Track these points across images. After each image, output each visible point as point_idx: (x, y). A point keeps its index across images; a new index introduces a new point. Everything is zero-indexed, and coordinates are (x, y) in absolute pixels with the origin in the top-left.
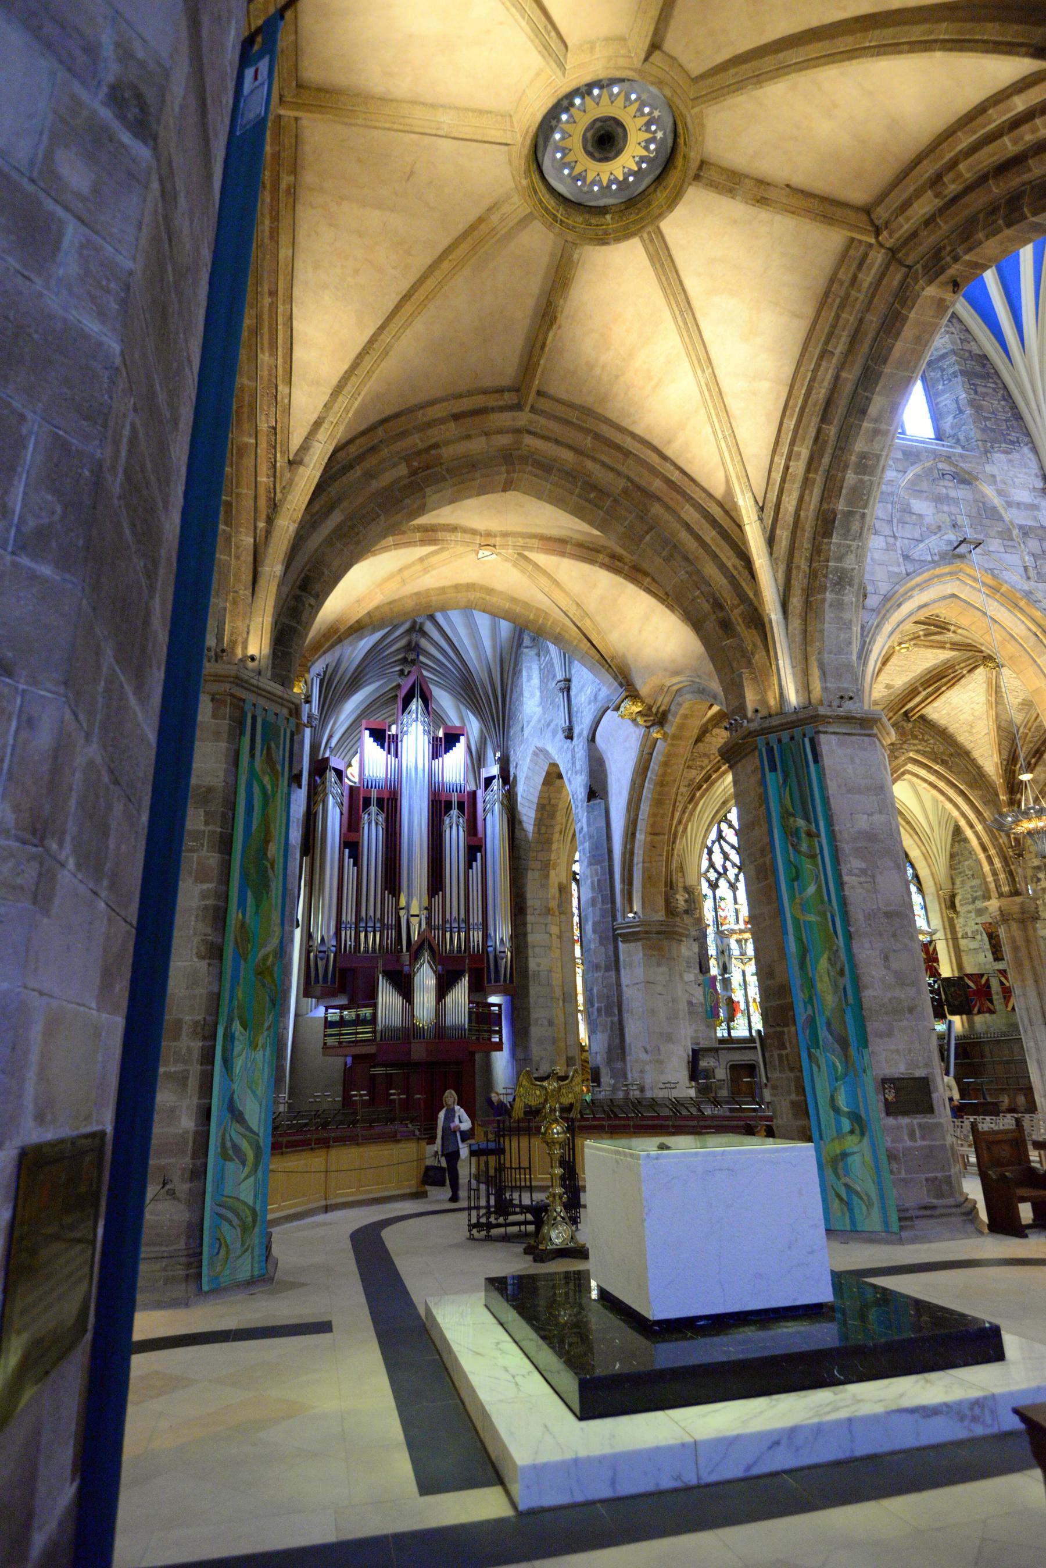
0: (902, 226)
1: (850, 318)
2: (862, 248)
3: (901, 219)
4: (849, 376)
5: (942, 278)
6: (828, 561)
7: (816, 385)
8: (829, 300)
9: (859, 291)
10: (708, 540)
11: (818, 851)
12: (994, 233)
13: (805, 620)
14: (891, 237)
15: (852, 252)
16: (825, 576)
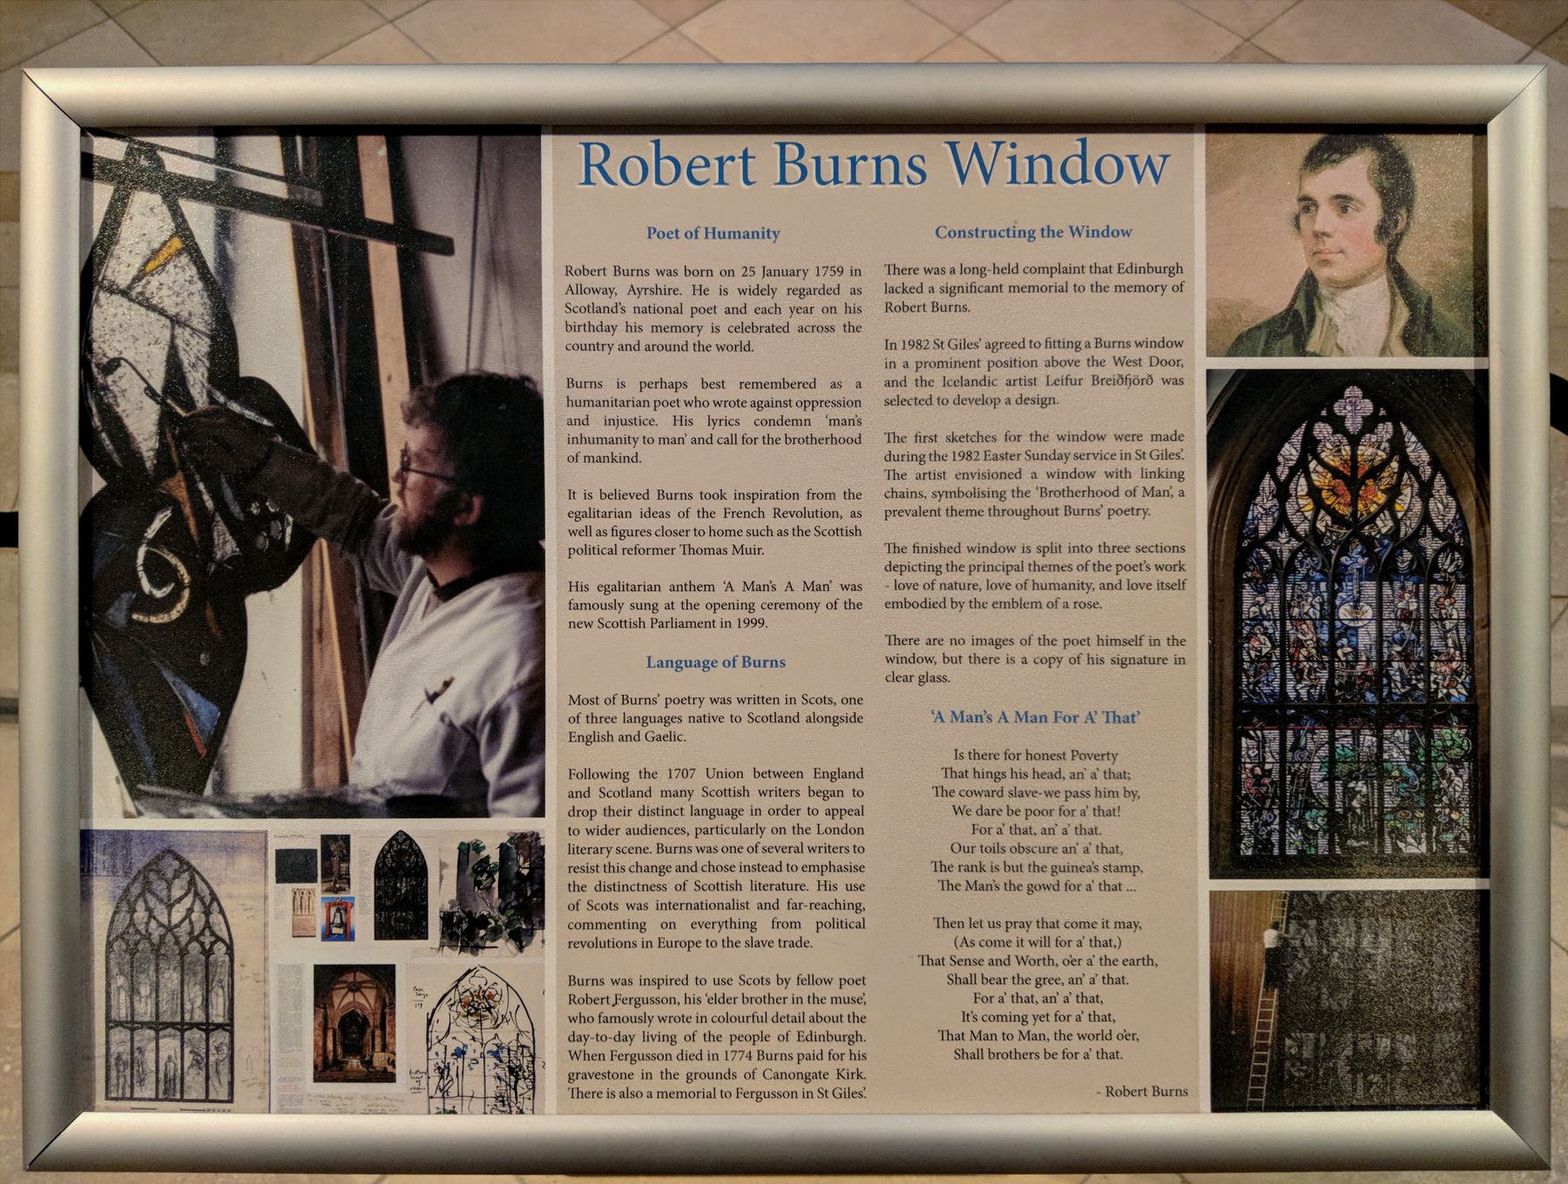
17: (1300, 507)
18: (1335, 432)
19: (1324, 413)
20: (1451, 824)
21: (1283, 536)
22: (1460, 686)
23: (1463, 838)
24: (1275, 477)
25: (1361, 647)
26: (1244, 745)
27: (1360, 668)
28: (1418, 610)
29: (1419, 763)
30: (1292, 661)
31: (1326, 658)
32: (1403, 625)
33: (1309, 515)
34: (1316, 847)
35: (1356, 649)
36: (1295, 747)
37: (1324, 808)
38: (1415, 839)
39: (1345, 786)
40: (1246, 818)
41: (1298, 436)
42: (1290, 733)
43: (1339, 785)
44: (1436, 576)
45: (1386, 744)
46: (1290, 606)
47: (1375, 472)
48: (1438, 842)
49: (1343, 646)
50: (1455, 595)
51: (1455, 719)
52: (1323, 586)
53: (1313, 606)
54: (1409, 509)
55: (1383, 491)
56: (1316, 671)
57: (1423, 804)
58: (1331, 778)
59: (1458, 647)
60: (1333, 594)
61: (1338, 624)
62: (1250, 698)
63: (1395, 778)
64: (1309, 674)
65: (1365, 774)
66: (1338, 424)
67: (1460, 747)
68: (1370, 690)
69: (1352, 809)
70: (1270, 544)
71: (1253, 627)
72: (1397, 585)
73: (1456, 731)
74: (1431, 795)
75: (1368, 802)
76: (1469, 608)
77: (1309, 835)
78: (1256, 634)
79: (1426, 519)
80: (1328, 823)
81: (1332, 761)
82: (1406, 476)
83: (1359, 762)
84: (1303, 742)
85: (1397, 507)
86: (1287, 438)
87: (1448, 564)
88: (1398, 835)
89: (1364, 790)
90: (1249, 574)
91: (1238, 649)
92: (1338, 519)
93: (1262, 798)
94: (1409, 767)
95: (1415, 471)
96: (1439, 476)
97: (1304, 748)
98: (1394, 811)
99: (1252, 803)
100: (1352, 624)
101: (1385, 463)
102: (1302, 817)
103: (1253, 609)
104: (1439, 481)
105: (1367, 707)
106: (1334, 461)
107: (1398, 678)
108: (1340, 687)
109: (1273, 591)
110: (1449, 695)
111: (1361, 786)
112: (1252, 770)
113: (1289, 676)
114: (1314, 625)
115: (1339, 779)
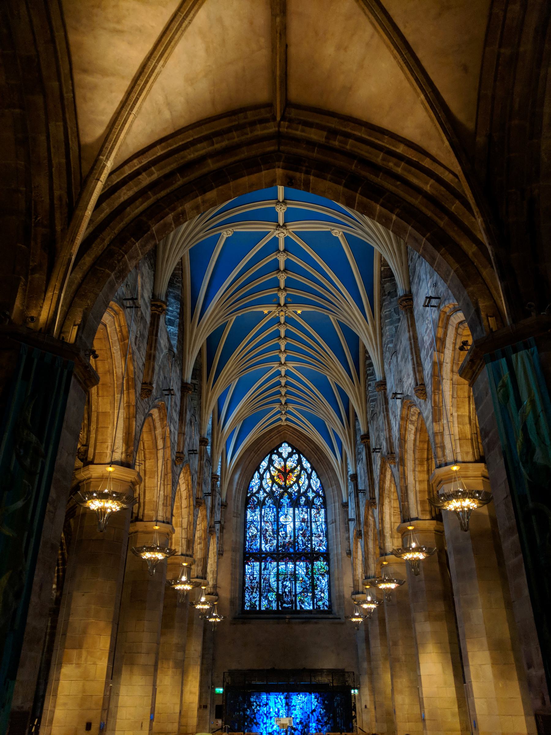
0: (297, 130)
1: (236, 138)
2: (268, 115)
3: (300, 127)
4: (211, 165)
5: (291, 173)
6: (126, 253)
7: (192, 149)
8: (233, 117)
9: (251, 132)
10: (55, 162)
11: (38, 471)
12: (336, 182)
13: (84, 278)
14: (287, 128)
15: (263, 110)
16: (119, 261)
18: (279, 458)
19: (275, 451)
20: (321, 599)
21: (261, 492)
23: (326, 604)
24: (259, 473)
25: (288, 531)
26: (247, 568)
28: (308, 518)
29: (309, 575)
31: (275, 536)
33: (270, 485)
34: (272, 607)
35: (286, 533)
36: (265, 568)
37: (275, 592)
38: (308, 603)
39: (282, 583)
40: (247, 596)
41: (267, 459)
42: (263, 563)
43: (280, 582)
44: (314, 506)
46: (264, 517)
47: (292, 470)
48: (317, 605)
49: (281, 531)
51: (322, 558)
52: (275, 510)
53: (271, 517)
54: (304, 483)
58: (278, 580)
59: (322, 531)
61: (280, 523)
62: (249, 550)
63: (301, 580)
64: (270, 541)
65: (290, 579)
66: (280, 455)
67: (324, 569)
68: (291, 547)
69: (285, 592)
70: (257, 495)
71: (251, 524)
72: (300, 509)
73: (322, 562)
74: (314, 587)
75: (291, 589)
76: (326, 518)
77: (270, 602)
79: (309, 486)
80: (277, 598)
81: (278, 574)
82: (302, 472)
84: (267, 567)
85: (300, 482)
86: (263, 459)
88: (302, 602)
89: (289, 585)
90: (250, 506)
91: (245, 532)
93: (253, 588)
94: (306, 576)
95: (305, 470)
96: (314, 472)
97: (268, 569)
98: (300, 593)
99: (249, 590)
100: (284, 524)
101: (296, 467)
102: (267, 595)
103: (251, 518)
104: (314, 474)
105: (291, 554)
106: (279, 467)
107: (301, 543)
108: (281, 546)
109: (258, 511)
110: (319, 549)
111: (288, 584)
112: (249, 577)
113: (263, 542)
114: (272, 524)
115: (280, 581)
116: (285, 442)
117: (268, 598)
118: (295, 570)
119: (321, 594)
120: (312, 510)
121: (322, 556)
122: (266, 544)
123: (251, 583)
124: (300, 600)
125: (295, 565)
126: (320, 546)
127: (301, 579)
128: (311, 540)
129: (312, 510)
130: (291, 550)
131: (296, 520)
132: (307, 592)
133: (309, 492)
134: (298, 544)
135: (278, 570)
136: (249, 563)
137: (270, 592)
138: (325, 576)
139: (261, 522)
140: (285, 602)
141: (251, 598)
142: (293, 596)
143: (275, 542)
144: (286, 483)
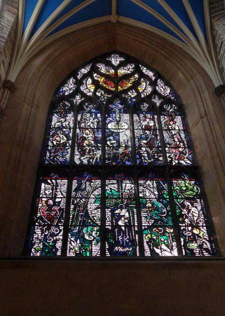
17: (88, 88)
20: (194, 238)
21: (78, 97)
22: (185, 159)
25: (121, 140)
26: (43, 187)
27: (121, 150)
28: (155, 125)
30: (78, 147)
32: (146, 131)
34: (91, 252)
35: (118, 142)
36: (78, 189)
37: (97, 225)
38: (168, 246)
39: (112, 212)
40: (38, 231)
42: (75, 182)
45: (141, 188)
46: (80, 123)
49: (110, 140)
50: (175, 120)
52: (99, 115)
53: (92, 123)
54: (145, 89)
55: (130, 84)
56: (93, 151)
57: (172, 224)
58: (103, 207)
59: (181, 141)
60: (104, 119)
63: (149, 207)
66: (109, 64)
68: (128, 160)
72: (142, 116)
74: (177, 219)
75: (129, 221)
78: (58, 134)
79: (155, 92)
82: (142, 79)
83: (122, 198)
85: (139, 89)
86: (84, 66)
87: (170, 109)
88: (154, 243)
89: (127, 215)
92: (107, 91)
93: (51, 219)
94: (158, 200)
95: (147, 78)
99: (45, 222)
101: (132, 74)
103: (58, 124)
107: (146, 155)
108: (109, 159)
109: (70, 117)
110: (179, 162)
111: (124, 212)
112: (46, 202)
113: (77, 152)
115: (108, 208)
116: (115, 52)
117: (83, 237)
118: (138, 192)
119: (192, 229)
120: (162, 117)
121: (185, 173)
122: (83, 153)
123: (50, 208)
124: (151, 239)
125: (137, 185)
126: (180, 159)
127: (150, 205)
128: (165, 153)
129: (162, 117)
130: (128, 163)
131: (136, 127)
132: (164, 227)
133: (155, 98)
134: (141, 155)
135: (104, 191)
136: (49, 181)
137: (87, 226)
138: (196, 202)
139: (75, 128)
140: (117, 244)
141: (46, 236)
142: (136, 232)
143: (99, 153)
144: (117, 89)
